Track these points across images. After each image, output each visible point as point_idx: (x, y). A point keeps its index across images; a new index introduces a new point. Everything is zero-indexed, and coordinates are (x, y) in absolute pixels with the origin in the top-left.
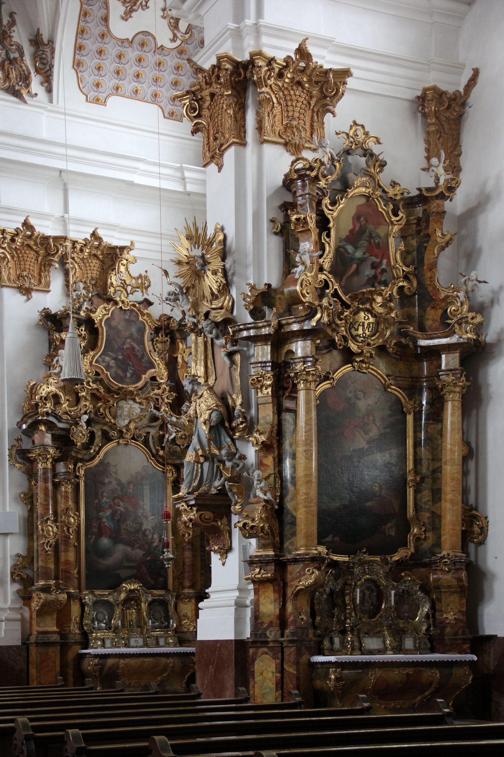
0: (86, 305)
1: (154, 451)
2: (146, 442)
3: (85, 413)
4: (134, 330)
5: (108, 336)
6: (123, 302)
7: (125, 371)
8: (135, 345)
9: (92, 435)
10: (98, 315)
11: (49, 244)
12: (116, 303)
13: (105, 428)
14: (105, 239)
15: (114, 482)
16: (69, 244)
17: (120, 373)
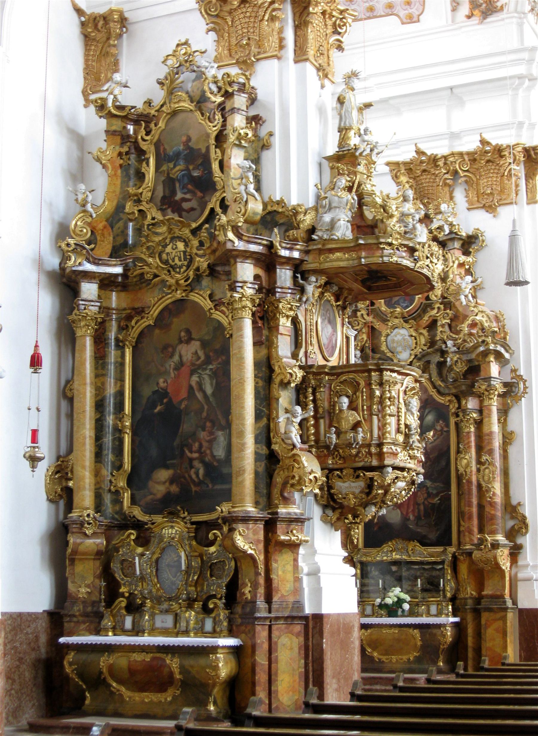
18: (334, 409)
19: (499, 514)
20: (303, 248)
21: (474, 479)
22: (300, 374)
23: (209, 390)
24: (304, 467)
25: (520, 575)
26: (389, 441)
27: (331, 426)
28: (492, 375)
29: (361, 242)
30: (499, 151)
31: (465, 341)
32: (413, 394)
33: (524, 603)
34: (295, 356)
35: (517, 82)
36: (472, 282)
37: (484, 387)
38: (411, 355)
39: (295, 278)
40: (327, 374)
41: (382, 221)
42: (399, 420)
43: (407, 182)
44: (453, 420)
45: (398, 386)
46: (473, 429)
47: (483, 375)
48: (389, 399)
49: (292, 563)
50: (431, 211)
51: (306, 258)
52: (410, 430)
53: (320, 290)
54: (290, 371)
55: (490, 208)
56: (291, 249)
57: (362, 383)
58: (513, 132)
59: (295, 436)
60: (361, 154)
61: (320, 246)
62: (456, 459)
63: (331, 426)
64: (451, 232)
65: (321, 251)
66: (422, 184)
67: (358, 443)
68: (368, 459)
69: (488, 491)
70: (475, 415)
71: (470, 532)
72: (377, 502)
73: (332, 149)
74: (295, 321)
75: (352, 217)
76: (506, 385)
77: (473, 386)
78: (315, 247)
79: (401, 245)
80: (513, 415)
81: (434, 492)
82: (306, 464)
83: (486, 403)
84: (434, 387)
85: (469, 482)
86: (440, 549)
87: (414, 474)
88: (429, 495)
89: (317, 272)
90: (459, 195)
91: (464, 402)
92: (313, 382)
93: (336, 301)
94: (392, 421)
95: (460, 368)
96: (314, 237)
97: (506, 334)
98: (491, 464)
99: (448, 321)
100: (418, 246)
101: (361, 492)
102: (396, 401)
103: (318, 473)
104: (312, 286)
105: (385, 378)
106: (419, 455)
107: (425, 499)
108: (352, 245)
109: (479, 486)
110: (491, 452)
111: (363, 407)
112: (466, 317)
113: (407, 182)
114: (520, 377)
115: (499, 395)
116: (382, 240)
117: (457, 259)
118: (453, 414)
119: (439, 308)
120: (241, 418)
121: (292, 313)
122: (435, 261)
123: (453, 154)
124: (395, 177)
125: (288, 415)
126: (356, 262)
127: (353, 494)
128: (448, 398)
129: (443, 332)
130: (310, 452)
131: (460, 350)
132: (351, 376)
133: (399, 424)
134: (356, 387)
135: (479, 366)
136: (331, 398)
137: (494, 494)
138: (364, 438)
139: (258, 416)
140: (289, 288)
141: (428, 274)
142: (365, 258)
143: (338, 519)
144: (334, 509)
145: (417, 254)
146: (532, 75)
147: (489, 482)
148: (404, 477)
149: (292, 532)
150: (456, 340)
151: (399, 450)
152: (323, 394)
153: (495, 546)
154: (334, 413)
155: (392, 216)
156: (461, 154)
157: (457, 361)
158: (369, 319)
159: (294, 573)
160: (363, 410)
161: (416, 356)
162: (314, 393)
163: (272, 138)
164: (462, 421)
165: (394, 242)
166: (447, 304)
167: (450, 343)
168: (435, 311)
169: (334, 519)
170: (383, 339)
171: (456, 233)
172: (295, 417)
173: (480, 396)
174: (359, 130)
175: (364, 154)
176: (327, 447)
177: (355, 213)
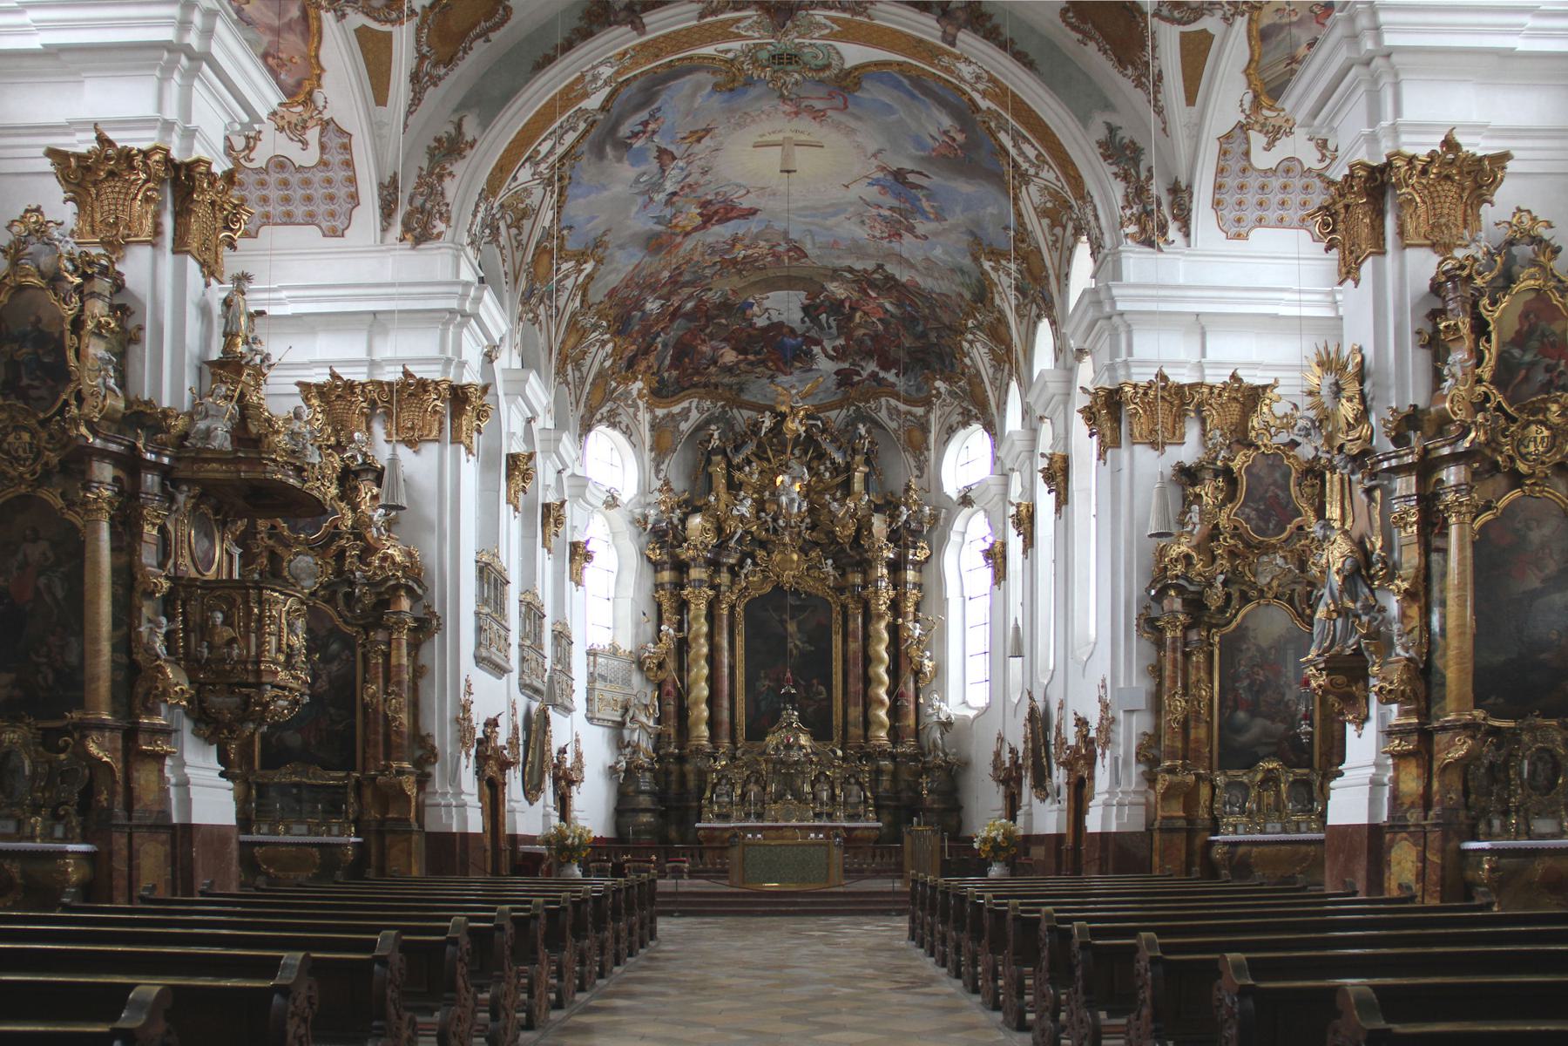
15: (1254, 648)
18: (207, 624)
23: (60, 594)
42: (280, 640)
45: (280, 606)
48: (269, 617)
55: (411, 443)
57: (239, 600)
59: (159, 646)
63: (202, 640)
92: (183, 594)
120: (97, 625)
132: (227, 591)
134: (232, 604)
138: (240, 655)
139: (116, 624)
162: (183, 606)
172: (160, 628)
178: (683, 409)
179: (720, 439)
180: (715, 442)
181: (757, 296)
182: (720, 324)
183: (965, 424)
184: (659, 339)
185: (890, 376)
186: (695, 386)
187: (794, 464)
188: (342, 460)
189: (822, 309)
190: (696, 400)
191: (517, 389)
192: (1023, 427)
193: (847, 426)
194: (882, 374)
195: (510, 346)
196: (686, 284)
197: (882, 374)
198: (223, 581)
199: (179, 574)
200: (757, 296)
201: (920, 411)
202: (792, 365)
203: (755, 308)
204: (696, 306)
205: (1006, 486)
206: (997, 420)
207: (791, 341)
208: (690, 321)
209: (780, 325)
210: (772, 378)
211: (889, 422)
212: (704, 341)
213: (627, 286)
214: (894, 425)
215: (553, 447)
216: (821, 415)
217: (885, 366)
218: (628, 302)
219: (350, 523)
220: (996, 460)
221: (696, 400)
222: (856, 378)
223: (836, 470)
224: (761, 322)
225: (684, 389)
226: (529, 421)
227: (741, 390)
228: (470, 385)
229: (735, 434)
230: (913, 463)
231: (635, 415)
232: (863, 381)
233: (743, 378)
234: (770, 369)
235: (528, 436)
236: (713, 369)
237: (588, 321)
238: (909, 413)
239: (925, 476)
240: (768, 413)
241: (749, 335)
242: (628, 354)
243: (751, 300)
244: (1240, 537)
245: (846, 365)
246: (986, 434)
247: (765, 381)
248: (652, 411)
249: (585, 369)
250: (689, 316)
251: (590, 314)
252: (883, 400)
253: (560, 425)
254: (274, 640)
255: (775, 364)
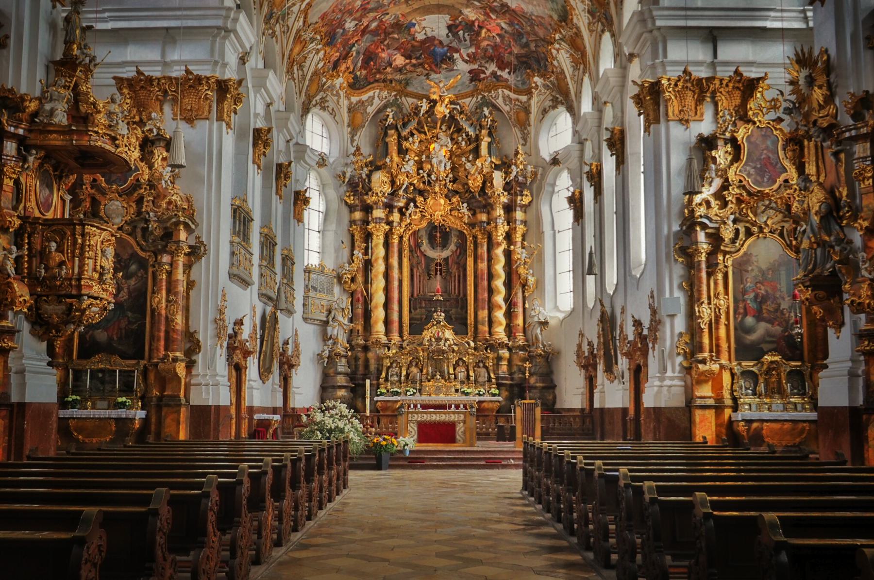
0: (730, 127)
1: (788, 242)
2: (781, 235)
3: (732, 214)
4: (769, 143)
5: (748, 150)
6: (760, 121)
7: (763, 177)
8: (770, 155)
9: (737, 231)
10: (741, 135)
11: (703, 84)
12: (754, 123)
13: (747, 225)
14: (745, 74)
16: (717, 82)
17: (759, 178)
18: (45, 251)
19: (179, 338)
20: (26, 127)
21: (163, 312)
22: (18, 222)
24: (16, 292)
25: (193, 382)
26: (86, 276)
27: (41, 263)
28: (181, 239)
29: (74, 128)
30: (199, 79)
31: (163, 214)
32: (109, 244)
33: (195, 401)
34: (15, 208)
35: (216, 31)
36: (171, 172)
37: (174, 248)
38: (122, 220)
39: (18, 150)
40: (41, 224)
41: (92, 114)
42: (96, 262)
43: (129, 94)
44: (150, 270)
45: (97, 237)
46: (164, 277)
47: (174, 239)
48: (89, 246)
49: (2, 364)
50: (144, 117)
51: (29, 136)
52: (104, 270)
53: (40, 161)
54: (10, 219)
55: (190, 121)
56: (16, 127)
58: (209, 67)
60: (80, 63)
61: (41, 128)
62: (151, 298)
63: (41, 263)
64: (158, 134)
65: (41, 132)
66: (140, 96)
67: (62, 277)
68: (69, 290)
69: (173, 321)
70: (167, 267)
71: (158, 350)
72: (75, 322)
73: (59, 56)
74: (17, 182)
75: (68, 108)
76: (190, 247)
77: (166, 246)
78: (36, 128)
79: (105, 134)
80: (195, 268)
81: (134, 320)
82: (17, 290)
83: (174, 259)
84: (138, 244)
85: (160, 314)
86: (134, 362)
87: (106, 302)
88: (130, 323)
89: (38, 148)
90: (167, 108)
91: (159, 257)
92: (29, 229)
93: (54, 172)
94: (90, 262)
95: (158, 232)
96: (37, 120)
97: (194, 211)
98: (176, 302)
99: (152, 198)
100: (118, 137)
101: (62, 313)
102: (95, 248)
103: (27, 298)
104: (33, 157)
105: (86, 231)
106: (110, 289)
107: (126, 325)
108: (66, 129)
109: (167, 318)
110: (176, 294)
111: (67, 250)
112: (165, 196)
113: (129, 94)
114: (202, 243)
115: (185, 254)
116: (90, 129)
117: (162, 154)
118: (151, 265)
119: (145, 188)
121: (15, 176)
122: (132, 149)
123: (164, 78)
124: (120, 89)
125: (5, 252)
126: (69, 142)
127: (57, 314)
128: (148, 254)
129: (146, 206)
130: (24, 282)
131: (159, 220)
132: (60, 227)
133: (95, 266)
134: (63, 236)
135: (172, 232)
136: (42, 242)
137: (177, 323)
138: (67, 273)
140: (13, 157)
141: (127, 159)
142: (76, 140)
143: (44, 333)
144: (41, 326)
145: (117, 142)
146: (227, 28)
147: (173, 315)
148: (97, 304)
149: (3, 340)
150: (157, 212)
151: (94, 284)
152: (37, 239)
153: (175, 360)
154: (45, 253)
155: (99, 112)
156: (170, 78)
157: (156, 228)
158: (93, 191)
159: (4, 372)
160: (68, 253)
161: (126, 221)
162: (29, 238)
163: (8, 41)
164: (157, 270)
165: (100, 131)
166: (151, 185)
167: (151, 214)
168: (143, 190)
169: (41, 333)
170: (102, 207)
171: (162, 135)
172: (11, 254)
173: (172, 254)
174: (80, 44)
175: (83, 63)
176: (37, 279)
177: (71, 106)
178: (369, 97)
179: (393, 118)
180: (390, 120)
181: (418, 19)
182: (394, 38)
183: (554, 107)
184: (354, 49)
185: (505, 74)
186: (377, 81)
187: (442, 135)
188: (143, 132)
189: (460, 27)
190: (378, 91)
191: (261, 84)
192: (593, 109)
193: (476, 109)
194: (499, 72)
195: (257, 53)
196: (371, 10)
197: (499, 72)
198: (57, 219)
199: (27, 215)
200: (418, 19)
201: (524, 98)
202: (441, 67)
203: (417, 27)
204: (378, 26)
205: (582, 151)
206: (575, 104)
207: (439, 50)
208: (375, 36)
209: (433, 38)
210: (427, 75)
211: (503, 105)
212: (383, 50)
213: (333, 11)
214: (507, 108)
215: (284, 123)
216: (459, 101)
217: (501, 68)
218: (334, 23)
219: (147, 177)
220: (575, 132)
221: (378, 91)
222: (482, 76)
223: (469, 140)
224: (420, 37)
225: (370, 83)
226: (268, 105)
227: (407, 84)
228: (230, 80)
229: (403, 115)
230: (520, 135)
231: (338, 102)
232: (487, 78)
233: (409, 75)
234: (426, 69)
235: (268, 115)
236: (389, 70)
237: (307, 36)
238: (518, 100)
239: (528, 144)
240: (424, 100)
241: (413, 46)
242: (334, 59)
243: (414, 21)
244: (744, 187)
245: (476, 67)
246: (568, 114)
247: (423, 77)
248: (349, 99)
249: (305, 69)
250: (375, 33)
251: (310, 31)
252: (500, 91)
253: (289, 108)
254: (90, 262)
255: (430, 66)
